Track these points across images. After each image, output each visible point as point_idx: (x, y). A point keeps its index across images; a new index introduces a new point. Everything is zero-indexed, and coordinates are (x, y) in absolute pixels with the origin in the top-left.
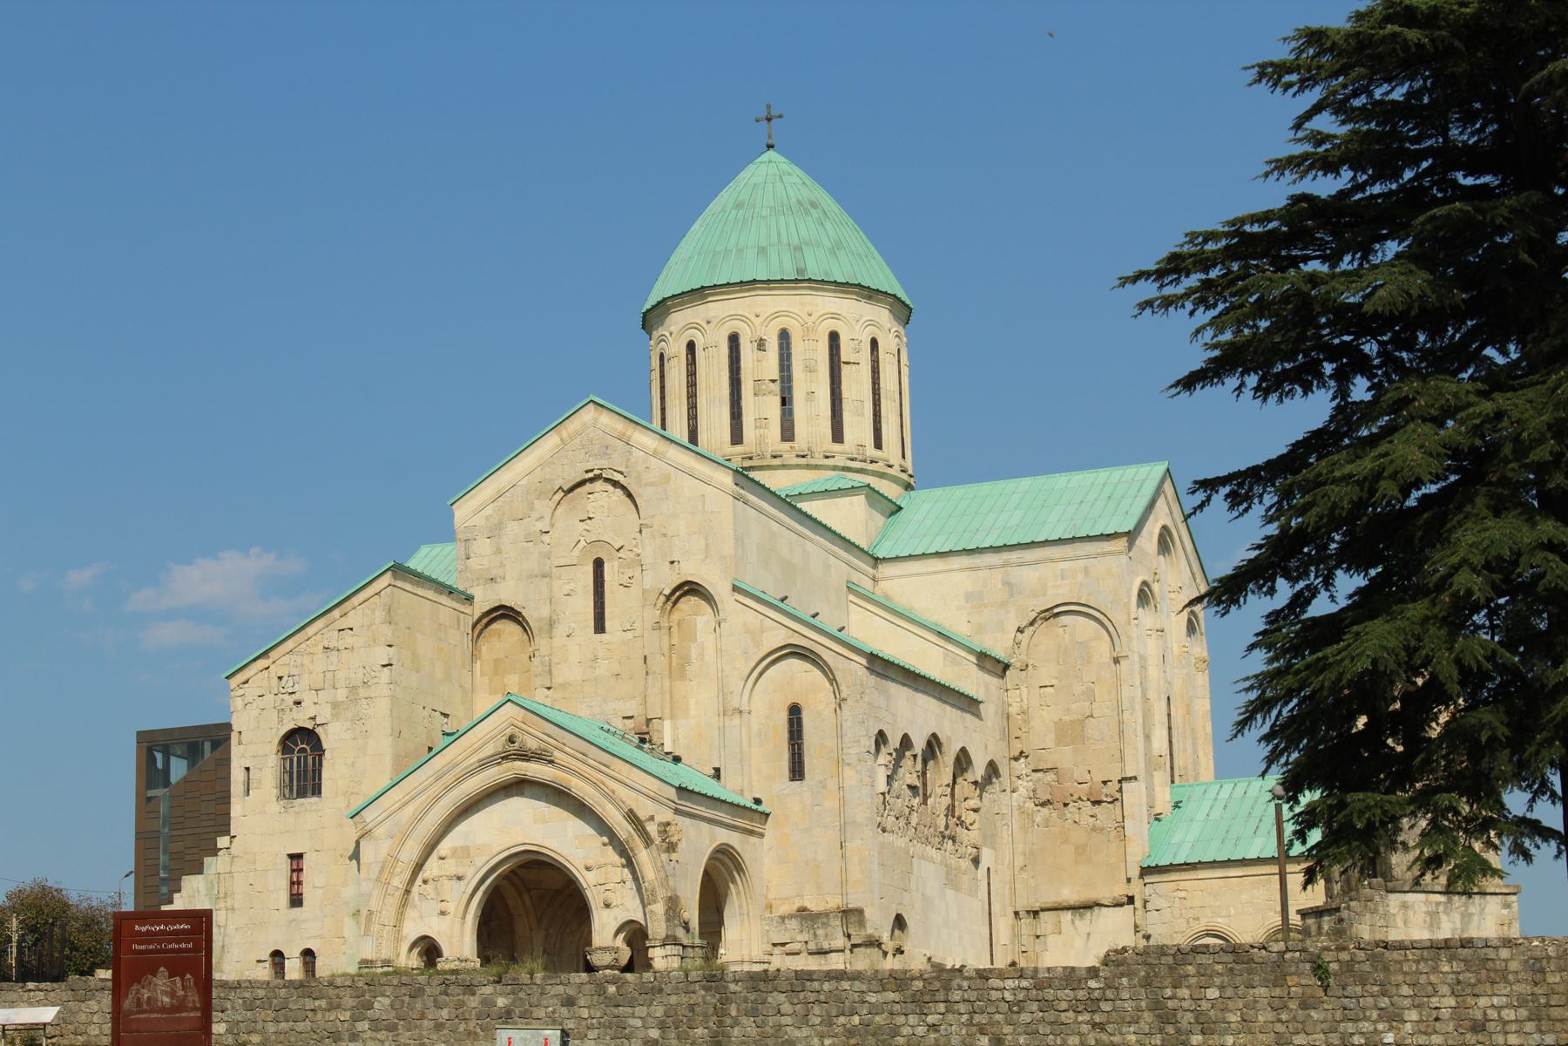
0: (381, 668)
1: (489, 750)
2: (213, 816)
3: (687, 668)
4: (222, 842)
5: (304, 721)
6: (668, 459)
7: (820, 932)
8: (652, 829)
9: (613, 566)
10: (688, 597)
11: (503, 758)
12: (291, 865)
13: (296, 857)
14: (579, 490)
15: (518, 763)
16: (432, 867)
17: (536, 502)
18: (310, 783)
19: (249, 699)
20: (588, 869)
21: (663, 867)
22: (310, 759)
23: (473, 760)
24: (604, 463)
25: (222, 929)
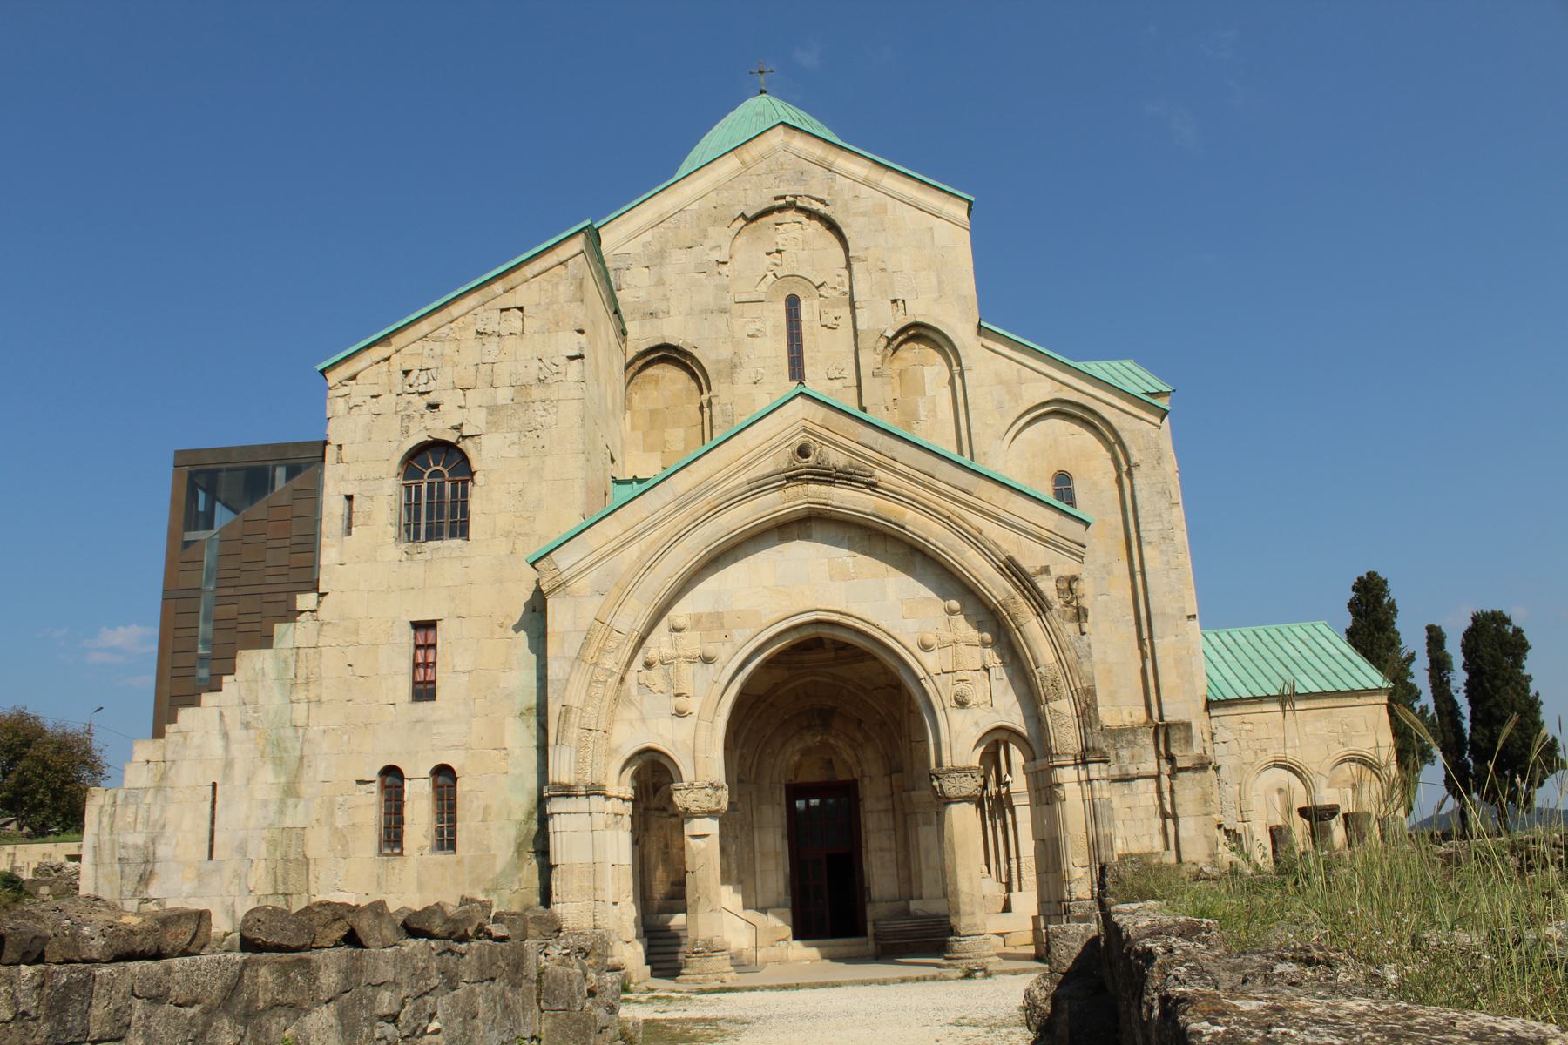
0: (565, 361)
2: (285, 570)
3: (915, 426)
4: (305, 601)
5: (444, 431)
6: (883, 187)
7: (1124, 753)
8: (1047, 586)
9: (812, 306)
10: (911, 345)
11: (788, 479)
12: (415, 638)
13: (424, 627)
14: (763, 220)
15: (813, 488)
16: (661, 640)
17: (710, 229)
18: (447, 521)
19: (354, 400)
20: (926, 648)
21: (1072, 644)
22: (448, 486)
23: (739, 481)
24: (800, 190)
25: (301, 731)
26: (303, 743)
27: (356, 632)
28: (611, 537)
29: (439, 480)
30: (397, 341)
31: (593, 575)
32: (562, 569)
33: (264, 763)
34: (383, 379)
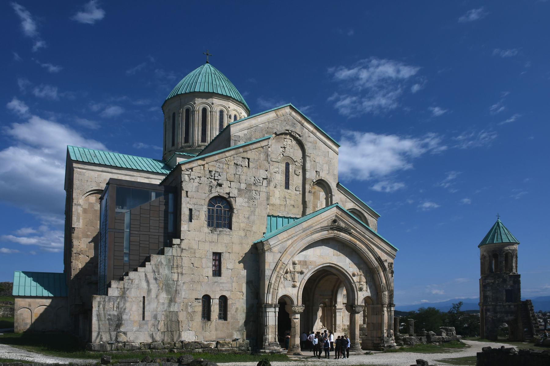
1: (325, 224)
5: (224, 194)
25: (175, 282)
26: (176, 286)
27: (195, 253)
28: (285, 237)
29: (220, 209)
30: (207, 160)
31: (279, 247)
32: (271, 244)
33: (162, 291)
34: (202, 172)
